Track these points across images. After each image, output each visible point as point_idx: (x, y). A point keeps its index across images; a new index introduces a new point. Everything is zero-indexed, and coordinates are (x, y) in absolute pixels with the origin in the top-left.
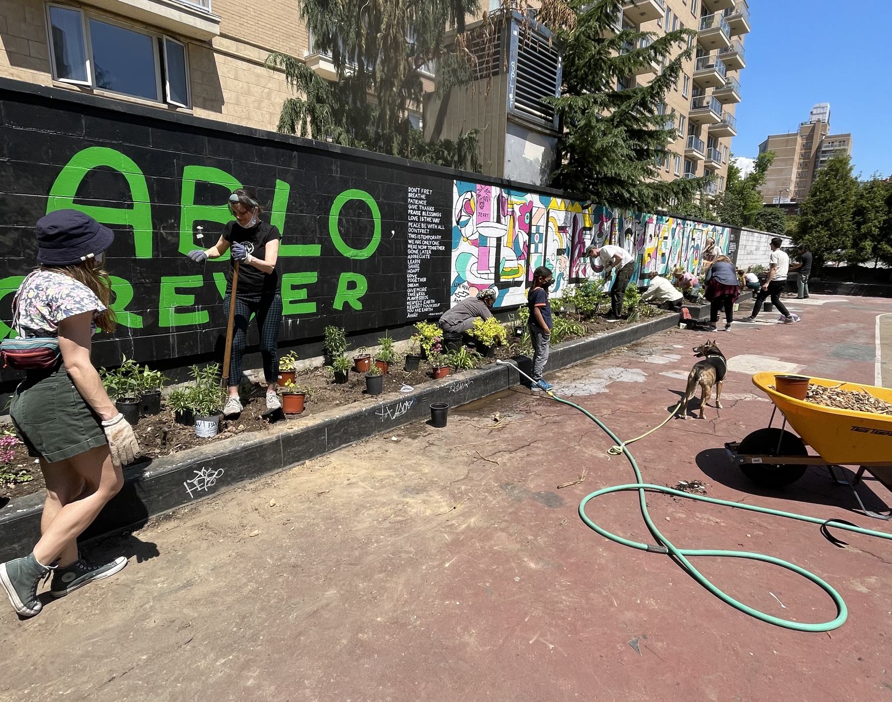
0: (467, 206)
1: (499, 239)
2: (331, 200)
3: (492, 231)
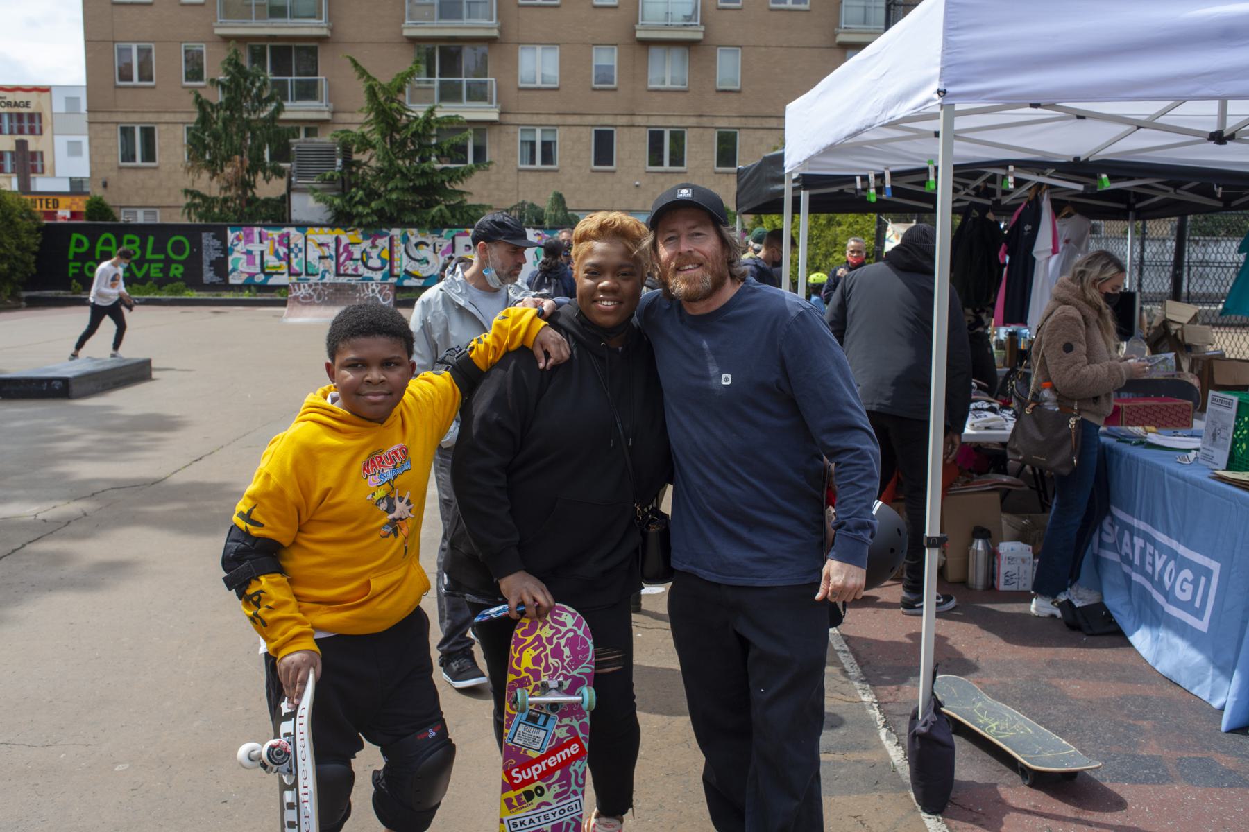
0: (238, 238)
1: (262, 253)
2: (167, 241)
3: (256, 248)
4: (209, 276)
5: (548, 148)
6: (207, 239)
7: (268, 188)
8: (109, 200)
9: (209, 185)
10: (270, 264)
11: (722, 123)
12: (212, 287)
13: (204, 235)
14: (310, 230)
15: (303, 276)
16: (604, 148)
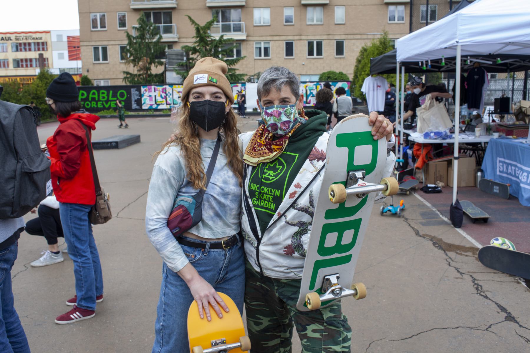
0: (146, 90)
1: (155, 96)
3: (153, 94)
4: (134, 106)
5: (266, 50)
6: (133, 91)
7: (156, 70)
8: (90, 76)
9: (133, 69)
10: (159, 100)
11: (338, 38)
12: (136, 110)
13: (132, 90)
14: (174, 86)
15: (172, 105)
16: (289, 49)
